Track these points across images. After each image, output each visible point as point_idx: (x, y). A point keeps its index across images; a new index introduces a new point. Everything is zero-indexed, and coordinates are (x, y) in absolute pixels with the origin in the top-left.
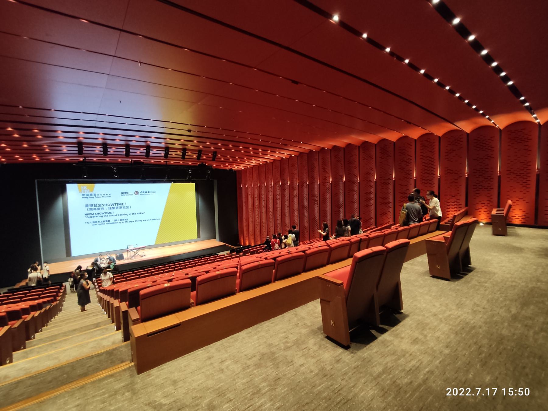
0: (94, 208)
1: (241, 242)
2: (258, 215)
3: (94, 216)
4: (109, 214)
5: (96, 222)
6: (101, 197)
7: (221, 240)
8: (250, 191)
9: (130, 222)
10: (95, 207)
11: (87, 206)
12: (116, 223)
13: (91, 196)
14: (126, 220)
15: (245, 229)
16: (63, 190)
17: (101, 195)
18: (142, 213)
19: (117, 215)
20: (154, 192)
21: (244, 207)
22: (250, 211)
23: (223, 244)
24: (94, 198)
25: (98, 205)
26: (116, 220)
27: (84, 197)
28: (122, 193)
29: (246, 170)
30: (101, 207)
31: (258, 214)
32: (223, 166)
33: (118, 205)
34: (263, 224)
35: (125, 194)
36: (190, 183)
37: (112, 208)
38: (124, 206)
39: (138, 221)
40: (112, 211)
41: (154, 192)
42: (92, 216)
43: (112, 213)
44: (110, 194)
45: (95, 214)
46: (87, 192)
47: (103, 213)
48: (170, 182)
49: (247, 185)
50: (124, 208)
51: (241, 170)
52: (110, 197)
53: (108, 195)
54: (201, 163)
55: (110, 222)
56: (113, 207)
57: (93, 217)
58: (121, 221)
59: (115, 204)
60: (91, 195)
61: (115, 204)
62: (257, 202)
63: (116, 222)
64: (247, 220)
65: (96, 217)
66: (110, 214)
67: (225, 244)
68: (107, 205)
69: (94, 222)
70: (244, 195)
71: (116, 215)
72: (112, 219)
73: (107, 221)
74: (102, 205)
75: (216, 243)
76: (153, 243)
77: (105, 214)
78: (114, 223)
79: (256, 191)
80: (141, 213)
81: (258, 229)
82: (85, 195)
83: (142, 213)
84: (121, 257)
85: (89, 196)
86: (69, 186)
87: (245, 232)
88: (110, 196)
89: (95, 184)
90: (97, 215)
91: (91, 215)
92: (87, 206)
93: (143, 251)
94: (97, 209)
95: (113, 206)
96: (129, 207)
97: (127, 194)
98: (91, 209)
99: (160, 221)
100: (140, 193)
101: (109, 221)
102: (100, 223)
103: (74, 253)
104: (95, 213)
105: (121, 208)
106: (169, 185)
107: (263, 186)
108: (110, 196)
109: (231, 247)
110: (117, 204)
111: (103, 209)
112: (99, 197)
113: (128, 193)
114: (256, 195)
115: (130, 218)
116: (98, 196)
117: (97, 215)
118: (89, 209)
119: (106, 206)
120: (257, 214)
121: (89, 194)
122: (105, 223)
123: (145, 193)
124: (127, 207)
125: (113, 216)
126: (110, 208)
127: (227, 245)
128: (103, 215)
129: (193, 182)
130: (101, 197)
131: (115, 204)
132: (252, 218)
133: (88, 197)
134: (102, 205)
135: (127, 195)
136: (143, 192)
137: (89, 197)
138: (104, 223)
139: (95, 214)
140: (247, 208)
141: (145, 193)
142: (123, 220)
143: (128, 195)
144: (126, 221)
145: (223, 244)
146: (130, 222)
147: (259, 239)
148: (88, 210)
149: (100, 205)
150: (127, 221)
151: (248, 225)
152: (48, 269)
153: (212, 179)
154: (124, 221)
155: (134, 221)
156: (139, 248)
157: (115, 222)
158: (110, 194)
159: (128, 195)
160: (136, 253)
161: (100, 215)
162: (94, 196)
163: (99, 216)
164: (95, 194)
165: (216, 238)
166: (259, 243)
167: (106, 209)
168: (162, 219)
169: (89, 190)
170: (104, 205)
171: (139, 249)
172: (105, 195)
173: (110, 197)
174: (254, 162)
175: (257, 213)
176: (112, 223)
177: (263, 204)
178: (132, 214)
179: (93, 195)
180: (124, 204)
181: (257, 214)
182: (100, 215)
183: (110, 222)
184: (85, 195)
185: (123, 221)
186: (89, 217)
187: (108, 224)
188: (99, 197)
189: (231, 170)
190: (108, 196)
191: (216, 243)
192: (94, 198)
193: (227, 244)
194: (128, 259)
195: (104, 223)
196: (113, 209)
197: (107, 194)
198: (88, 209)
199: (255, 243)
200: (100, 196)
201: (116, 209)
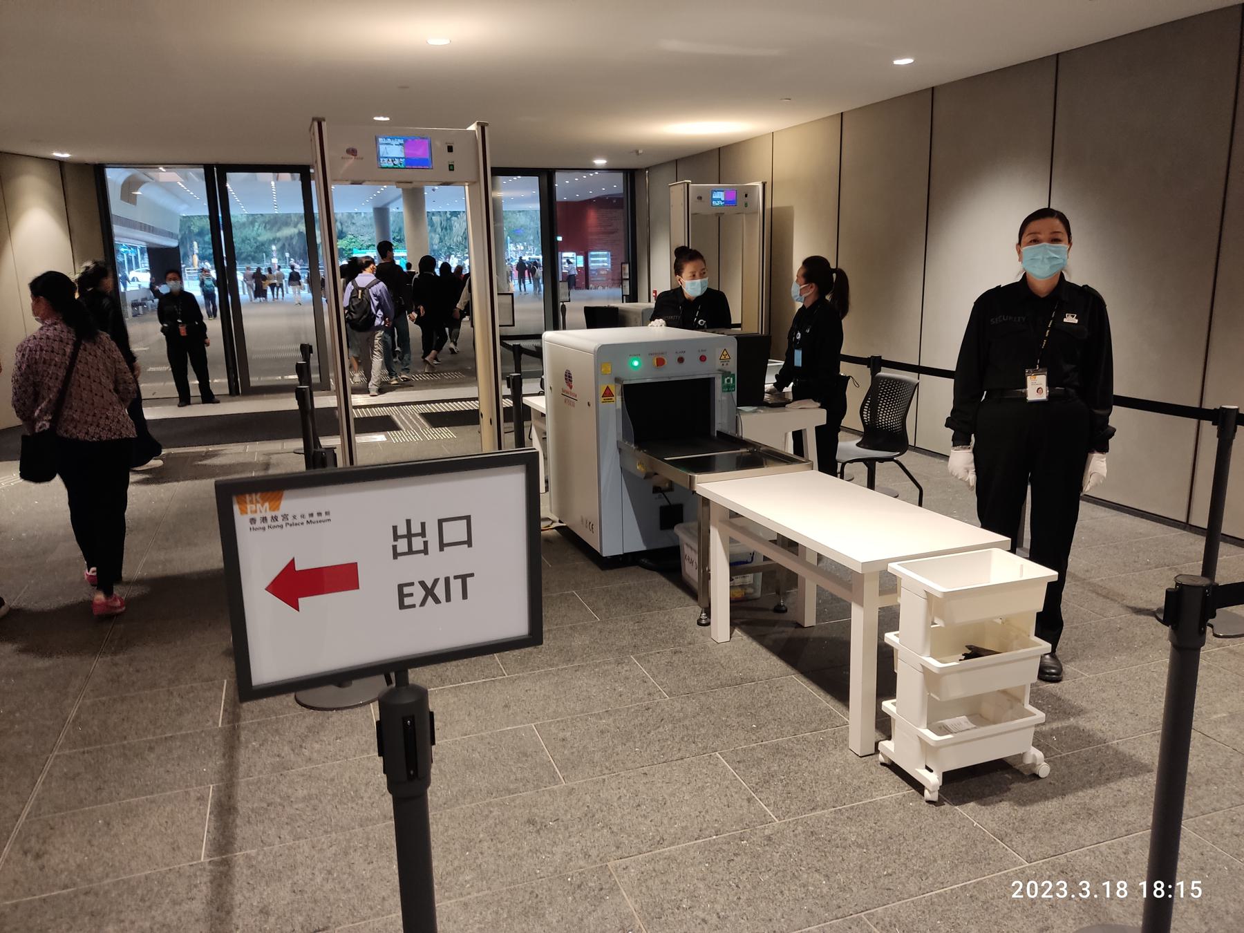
6: (302, 524)
17: (303, 516)
24: (282, 527)
27: (255, 526)
44: (327, 513)
52: (329, 520)
53: (324, 514)
88: (328, 517)
108: (328, 517)
116: (295, 521)
133: (266, 525)
137: (269, 527)
164: (285, 517)
172: (315, 515)
173: (329, 520)
179: (280, 519)
190: (324, 517)
192: (282, 527)
197: (319, 514)
200: (299, 520)
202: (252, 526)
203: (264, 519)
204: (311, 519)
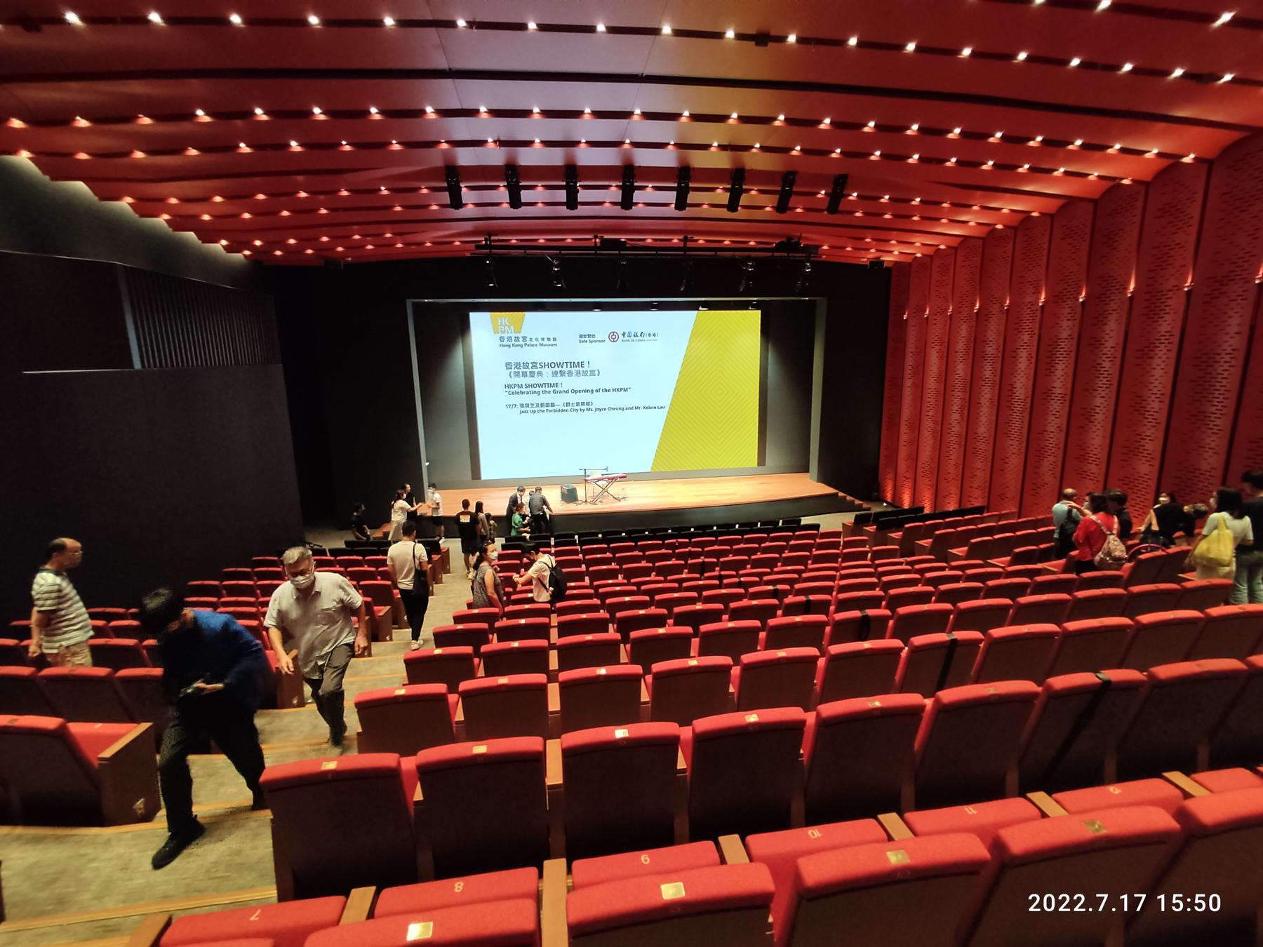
0: (523, 372)
1: (884, 491)
2: (962, 415)
3: (523, 390)
4: (554, 388)
5: (527, 406)
6: (536, 345)
7: (824, 478)
8: (936, 331)
9: (597, 409)
10: (525, 370)
11: (508, 366)
12: (567, 410)
13: (525, 342)
14: (588, 404)
15: (903, 453)
16: (463, 328)
17: (537, 339)
18: (626, 390)
19: (570, 391)
20: (654, 335)
21: (908, 383)
22: (930, 400)
23: (830, 490)
24: (522, 346)
25: (530, 366)
26: (568, 404)
27: (504, 343)
28: (581, 336)
29: (934, 256)
30: (536, 370)
31: (962, 407)
32: (854, 248)
33: (571, 367)
34: (978, 444)
35: (587, 339)
36: (747, 309)
37: (559, 375)
38: (584, 369)
39: (614, 409)
40: (558, 380)
41: (654, 335)
42: (518, 390)
43: (559, 385)
44: (555, 339)
45: (524, 386)
46: (509, 331)
47: (540, 386)
48: (693, 306)
49: (927, 312)
50: (585, 374)
51: (910, 264)
52: (556, 345)
53: (552, 340)
54: (785, 240)
55: (555, 408)
56: (561, 371)
57: (522, 393)
58: (578, 408)
59: (565, 364)
60: (517, 339)
61: (565, 364)
62: (961, 369)
63: (568, 408)
64: (916, 426)
65: (528, 393)
66: (555, 388)
67: (837, 494)
68: (548, 365)
69: (522, 405)
70: (911, 347)
71: (567, 392)
72: (559, 399)
73: (548, 405)
74: (538, 365)
75: (808, 485)
76: (646, 467)
77: (544, 389)
78: (562, 411)
79: (964, 330)
80: (621, 389)
81: (954, 456)
82: (506, 340)
83: (626, 390)
84: (570, 496)
85: (513, 342)
86: (475, 318)
87: (903, 465)
88: (555, 342)
89: (524, 313)
90: (528, 390)
91: (517, 389)
92: (508, 366)
93: (624, 486)
94: (528, 374)
95: (560, 369)
96: (596, 373)
97: (592, 339)
98: (517, 374)
99: (664, 412)
100: (621, 337)
101: (553, 405)
102: (533, 409)
103: (485, 475)
104: (526, 385)
105: (578, 373)
106: (691, 315)
107: (995, 309)
108: (555, 342)
109: (853, 502)
110: (569, 364)
111: (540, 374)
112: (532, 345)
113: (593, 336)
114: (961, 346)
115: (599, 400)
116: (532, 343)
117: (528, 390)
118: (512, 374)
119: (547, 367)
120: (955, 408)
121: (513, 336)
122: (545, 409)
123: (633, 336)
124: (592, 373)
125: (561, 392)
126: (556, 372)
127: (841, 494)
128: (541, 389)
129: (756, 306)
130: (536, 345)
131: (567, 363)
132: (935, 422)
133: (511, 343)
134: (538, 365)
135: (591, 342)
136: (629, 336)
137: (513, 345)
138: (542, 409)
139: (524, 386)
140: (920, 387)
141: (632, 338)
142: (583, 404)
143: (595, 341)
144: (588, 407)
145: (830, 490)
146: (597, 409)
147: (954, 490)
148: (511, 377)
149: (534, 364)
150: (590, 407)
151: (916, 442)
152: (437, 502)
153: (813, 296)
154: (585, 407)
155: (605, 409)
156: (612, 479)
157: (566, 408)
158: (555, 339)
159: (595, 341)
160: (604, 490)
161: (534, 389)
162: (523, 343)
163: (534, 393)
164: (524, 338)
165: (808, 472)
166: (952, 507)
167: (547, 376)
168: (670, 408)
169: (512, 327)
170: (543, 365)
171: (613, 480)
172: (546, 339)
173: (556, 345)
174: (972, 221)
175: (956, 404)
176: (559, 411)
177: (988, 373)
178: (601, 391)
179: (521, 339)
180: (586, 365)
181: (955, 408)
182: (534, 389)
183: (555, 408)
184: (506, 340)
185: (583, 407)
186: (513, 393)
187: (550, 411)
188: (532, 345)
189: (877, 263)
190: (552, 342)
191: (808, 485)
192: (522, 346)
193: (843, 492)
194: (586, 501)
195: (542, 409)
196: (561, 375)
197: (549, 339)
198: (511, 372)
199: (936, 503)
200: (534, 342)
201: (567, 375)
202: (501, 343)
203: (510, 339)
204: (543, 342)
